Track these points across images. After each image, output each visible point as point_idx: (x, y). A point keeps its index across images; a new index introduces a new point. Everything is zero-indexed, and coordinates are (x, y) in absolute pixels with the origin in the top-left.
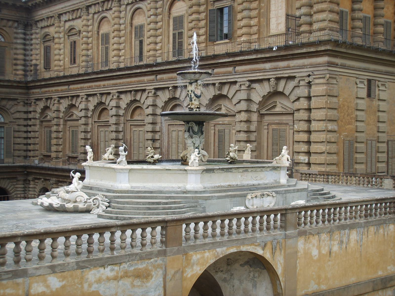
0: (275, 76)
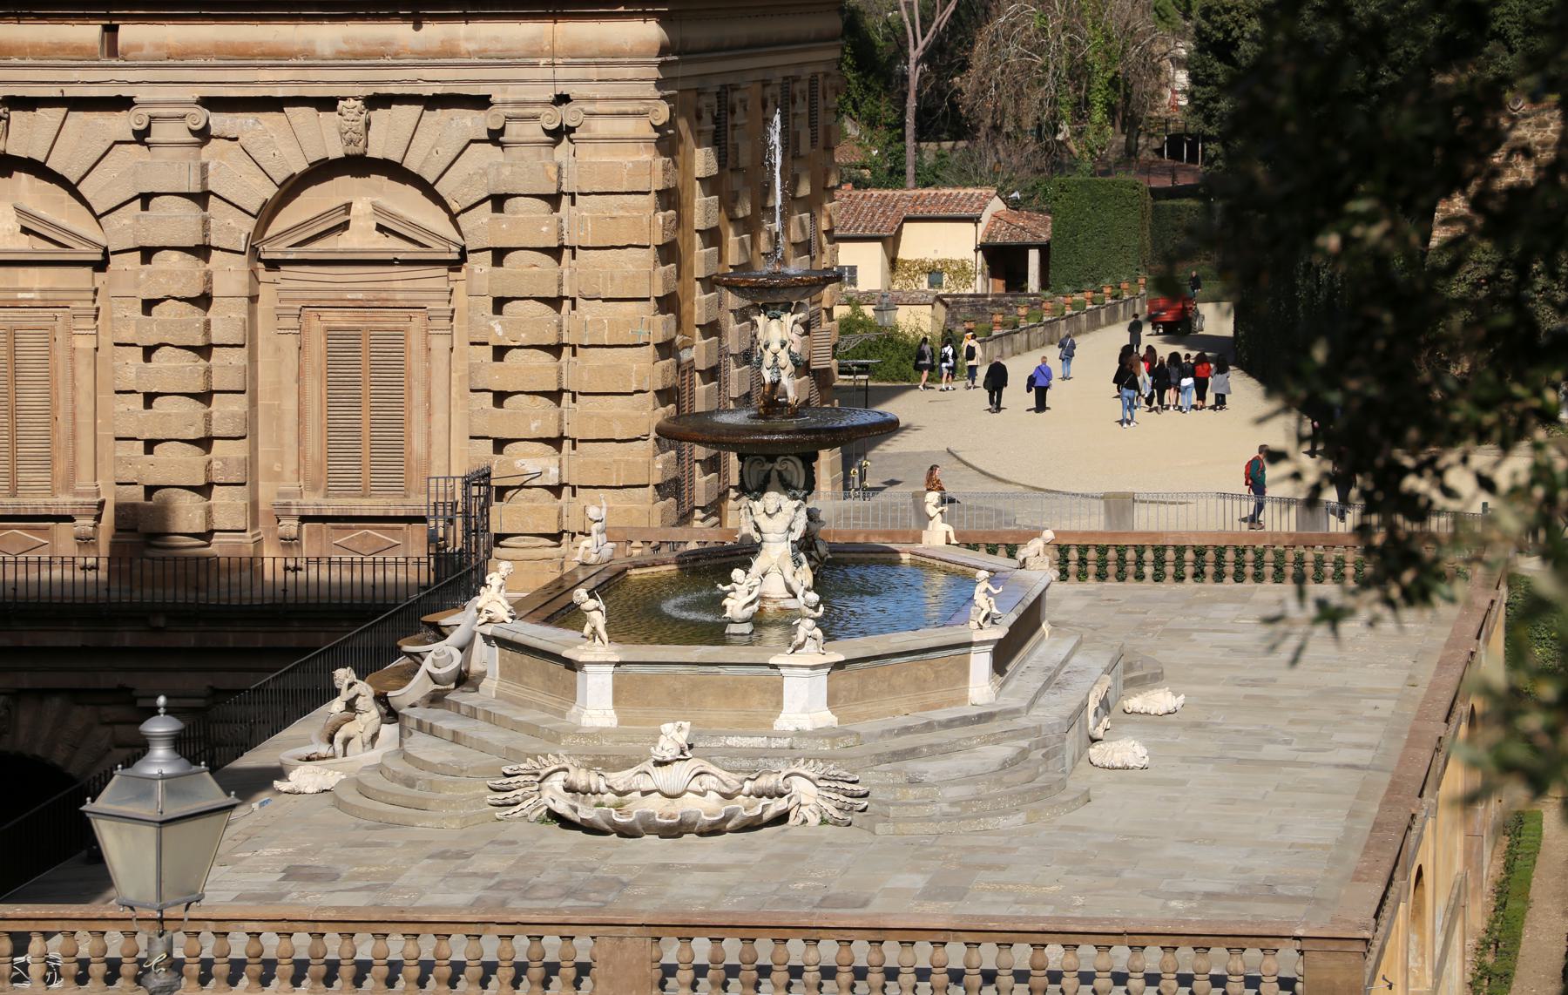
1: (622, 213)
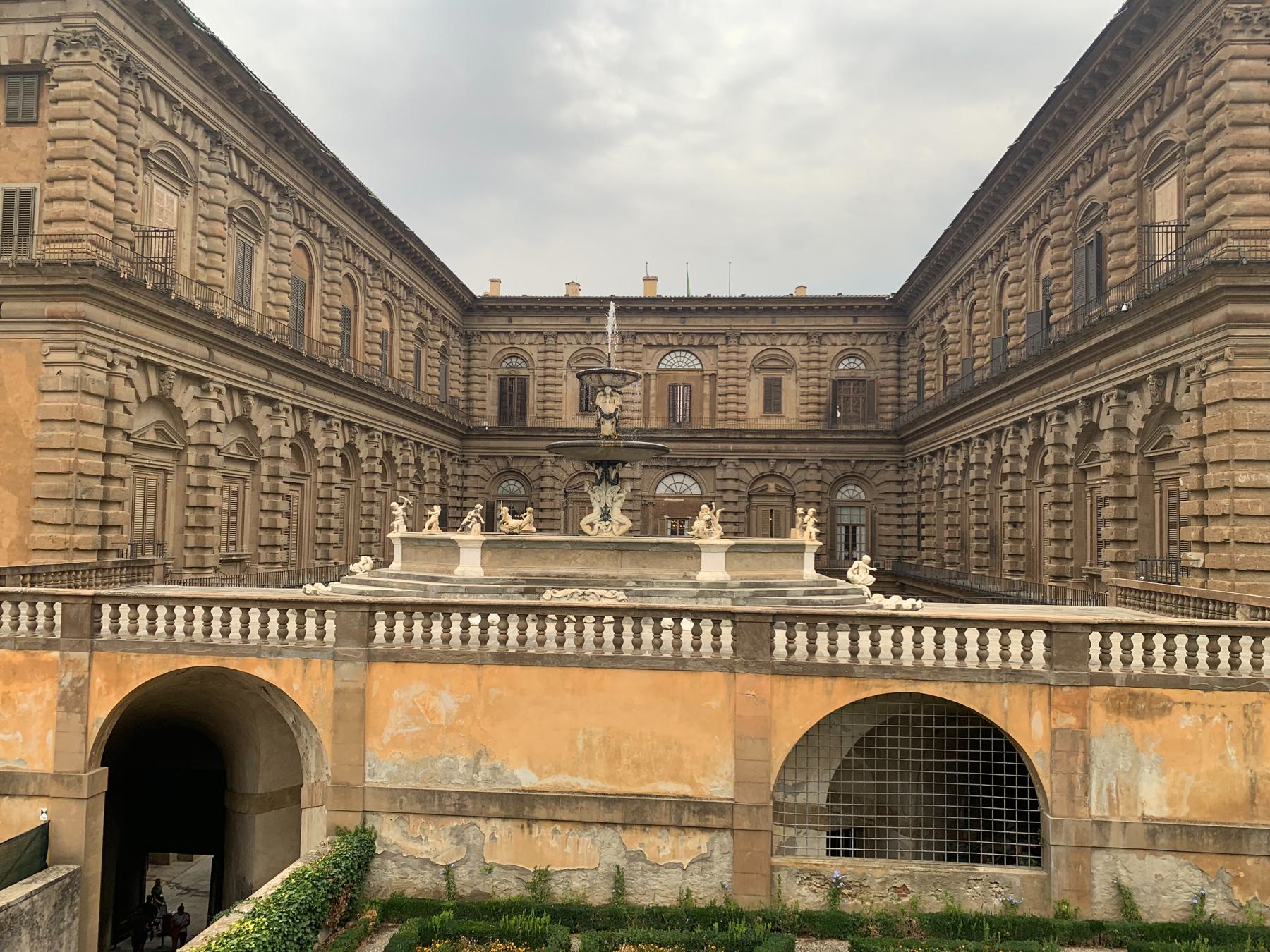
0: (1150, 370)
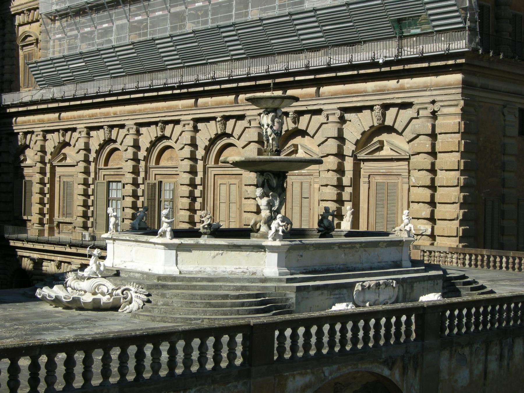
0: (381, 103)
1: (451, 140)
